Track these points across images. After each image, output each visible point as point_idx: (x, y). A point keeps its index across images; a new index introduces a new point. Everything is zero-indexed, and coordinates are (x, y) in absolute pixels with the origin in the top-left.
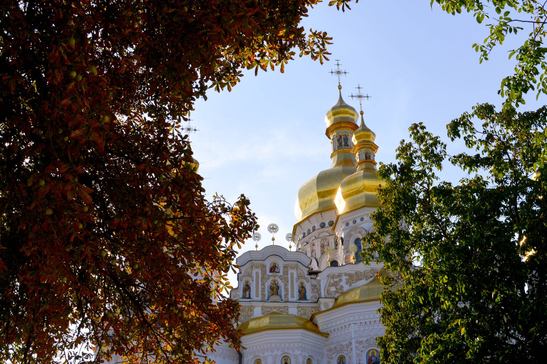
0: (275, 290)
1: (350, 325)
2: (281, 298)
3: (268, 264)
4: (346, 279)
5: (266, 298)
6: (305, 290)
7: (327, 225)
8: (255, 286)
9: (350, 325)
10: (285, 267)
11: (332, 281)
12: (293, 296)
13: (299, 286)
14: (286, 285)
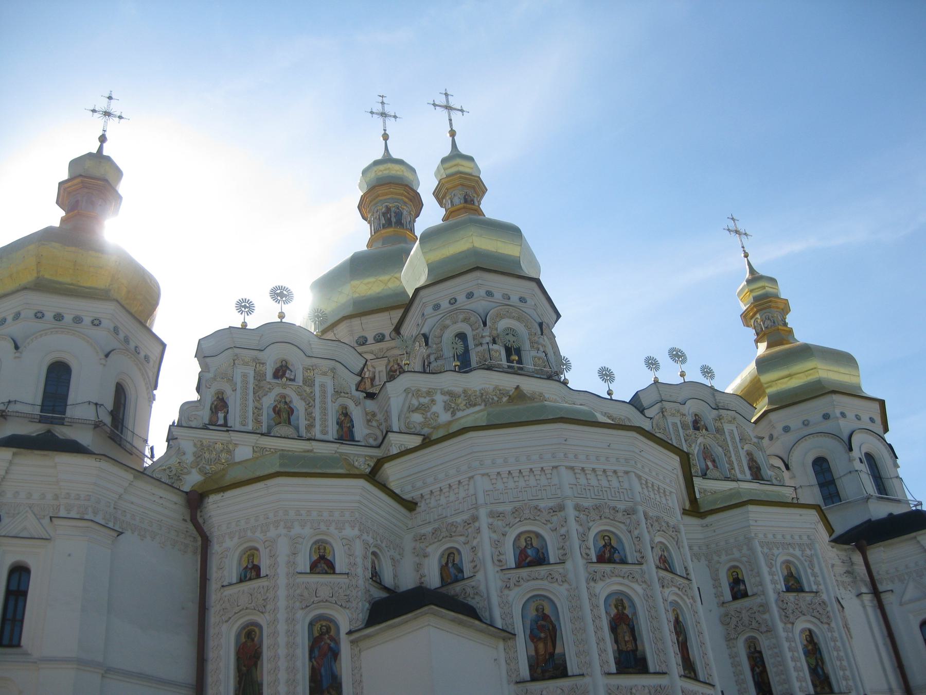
0: (284, 415)
2: (298, 432)
5: (264, 430)
6: (352, 421)
7: (370, 340)
9: (471, 478)
11: (415, 402)
12: (324, 432)
13: (337, 411)
14: (310, 405)
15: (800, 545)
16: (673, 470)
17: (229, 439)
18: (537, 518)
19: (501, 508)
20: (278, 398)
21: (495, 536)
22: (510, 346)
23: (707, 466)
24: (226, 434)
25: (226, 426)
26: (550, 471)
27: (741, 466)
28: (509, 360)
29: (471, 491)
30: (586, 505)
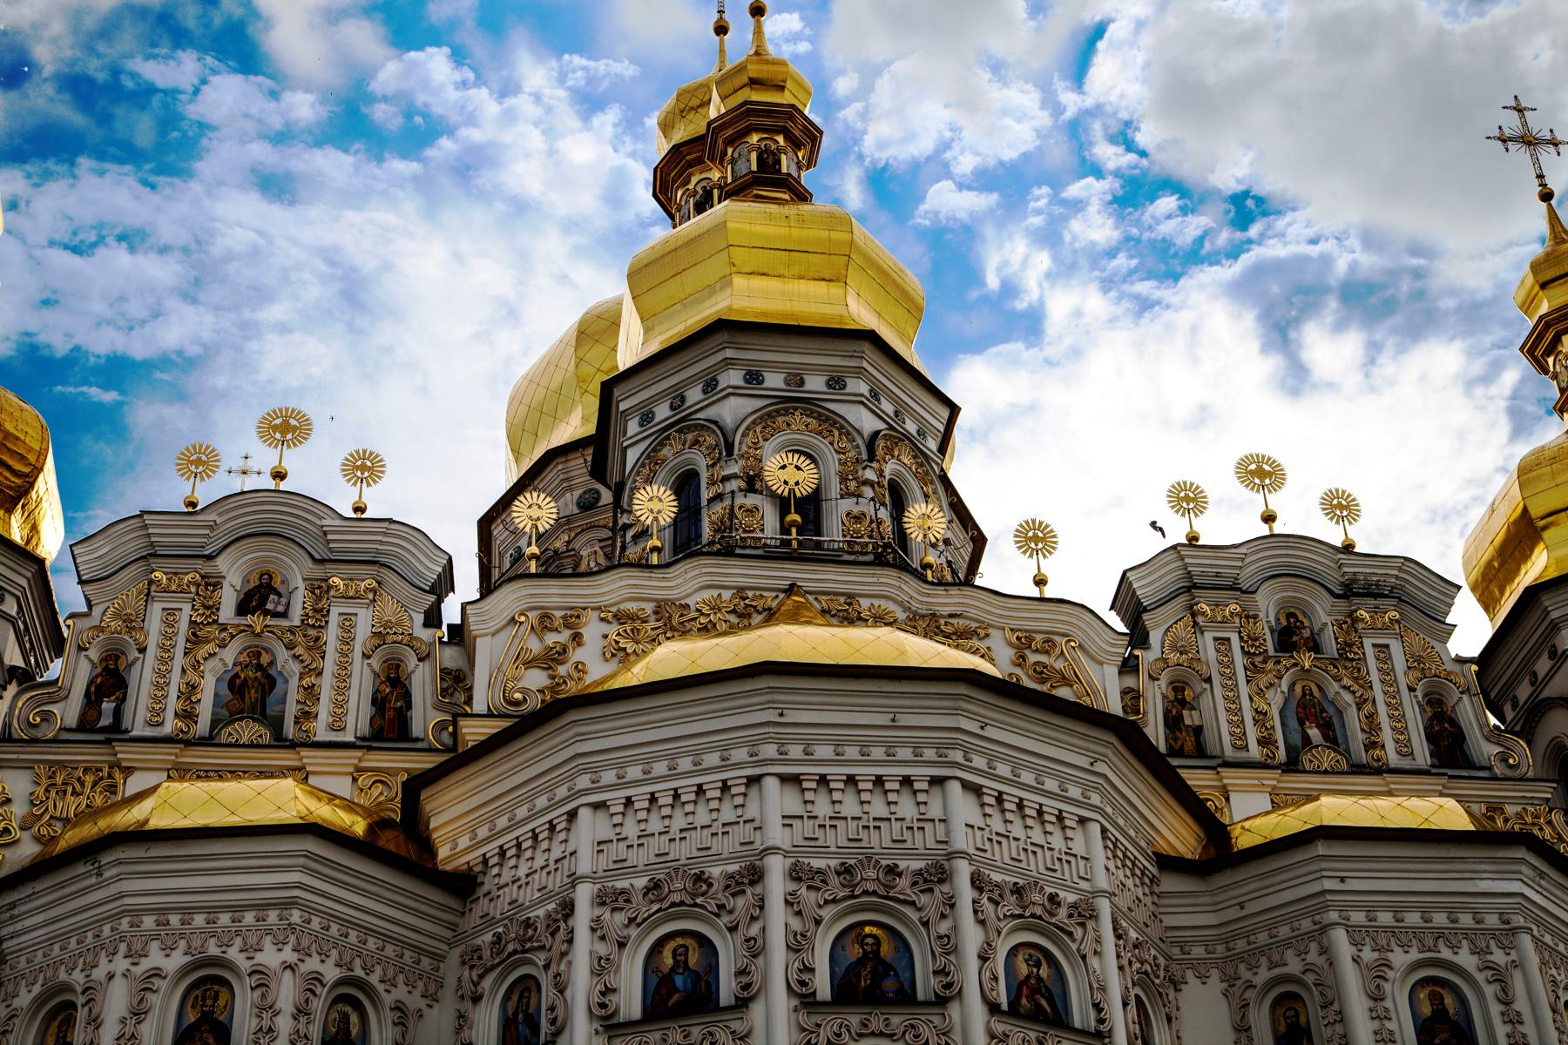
1: (572, 815)
3: (234, 573)
4: (606, 637)
6: (407, 697)
8: (148, 675)
10: (320, 589)
11: (535, 646)
14: (308, 671)
15: (1467, 934)
16: (1092, 764)
17: (111, 758)
18: (699, 901)
19: (622, 884)
20: (244, 658)
21: (602, 949)
22: (786, 494)
23: (1306, 740)
24: (105, 749)
25: (117, 731)
26: (742, 789)
27: (1401, 730)
28: (785, 530)
29: (570, 849)
30: (818, 863)
